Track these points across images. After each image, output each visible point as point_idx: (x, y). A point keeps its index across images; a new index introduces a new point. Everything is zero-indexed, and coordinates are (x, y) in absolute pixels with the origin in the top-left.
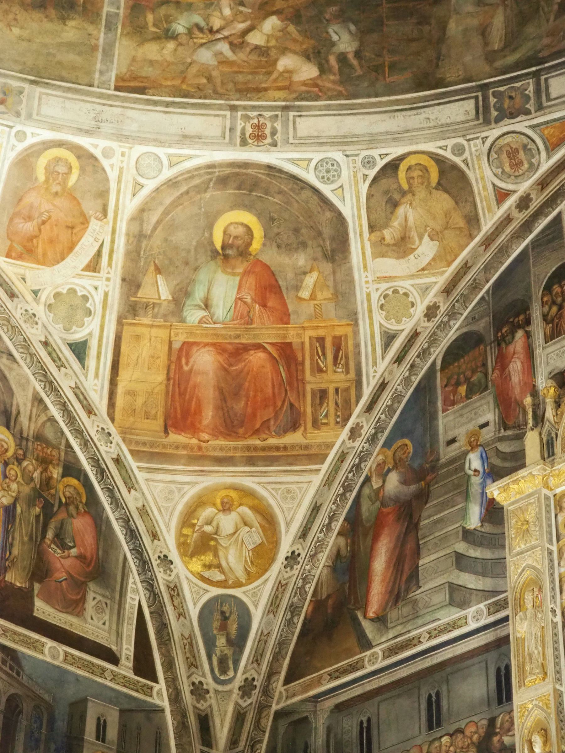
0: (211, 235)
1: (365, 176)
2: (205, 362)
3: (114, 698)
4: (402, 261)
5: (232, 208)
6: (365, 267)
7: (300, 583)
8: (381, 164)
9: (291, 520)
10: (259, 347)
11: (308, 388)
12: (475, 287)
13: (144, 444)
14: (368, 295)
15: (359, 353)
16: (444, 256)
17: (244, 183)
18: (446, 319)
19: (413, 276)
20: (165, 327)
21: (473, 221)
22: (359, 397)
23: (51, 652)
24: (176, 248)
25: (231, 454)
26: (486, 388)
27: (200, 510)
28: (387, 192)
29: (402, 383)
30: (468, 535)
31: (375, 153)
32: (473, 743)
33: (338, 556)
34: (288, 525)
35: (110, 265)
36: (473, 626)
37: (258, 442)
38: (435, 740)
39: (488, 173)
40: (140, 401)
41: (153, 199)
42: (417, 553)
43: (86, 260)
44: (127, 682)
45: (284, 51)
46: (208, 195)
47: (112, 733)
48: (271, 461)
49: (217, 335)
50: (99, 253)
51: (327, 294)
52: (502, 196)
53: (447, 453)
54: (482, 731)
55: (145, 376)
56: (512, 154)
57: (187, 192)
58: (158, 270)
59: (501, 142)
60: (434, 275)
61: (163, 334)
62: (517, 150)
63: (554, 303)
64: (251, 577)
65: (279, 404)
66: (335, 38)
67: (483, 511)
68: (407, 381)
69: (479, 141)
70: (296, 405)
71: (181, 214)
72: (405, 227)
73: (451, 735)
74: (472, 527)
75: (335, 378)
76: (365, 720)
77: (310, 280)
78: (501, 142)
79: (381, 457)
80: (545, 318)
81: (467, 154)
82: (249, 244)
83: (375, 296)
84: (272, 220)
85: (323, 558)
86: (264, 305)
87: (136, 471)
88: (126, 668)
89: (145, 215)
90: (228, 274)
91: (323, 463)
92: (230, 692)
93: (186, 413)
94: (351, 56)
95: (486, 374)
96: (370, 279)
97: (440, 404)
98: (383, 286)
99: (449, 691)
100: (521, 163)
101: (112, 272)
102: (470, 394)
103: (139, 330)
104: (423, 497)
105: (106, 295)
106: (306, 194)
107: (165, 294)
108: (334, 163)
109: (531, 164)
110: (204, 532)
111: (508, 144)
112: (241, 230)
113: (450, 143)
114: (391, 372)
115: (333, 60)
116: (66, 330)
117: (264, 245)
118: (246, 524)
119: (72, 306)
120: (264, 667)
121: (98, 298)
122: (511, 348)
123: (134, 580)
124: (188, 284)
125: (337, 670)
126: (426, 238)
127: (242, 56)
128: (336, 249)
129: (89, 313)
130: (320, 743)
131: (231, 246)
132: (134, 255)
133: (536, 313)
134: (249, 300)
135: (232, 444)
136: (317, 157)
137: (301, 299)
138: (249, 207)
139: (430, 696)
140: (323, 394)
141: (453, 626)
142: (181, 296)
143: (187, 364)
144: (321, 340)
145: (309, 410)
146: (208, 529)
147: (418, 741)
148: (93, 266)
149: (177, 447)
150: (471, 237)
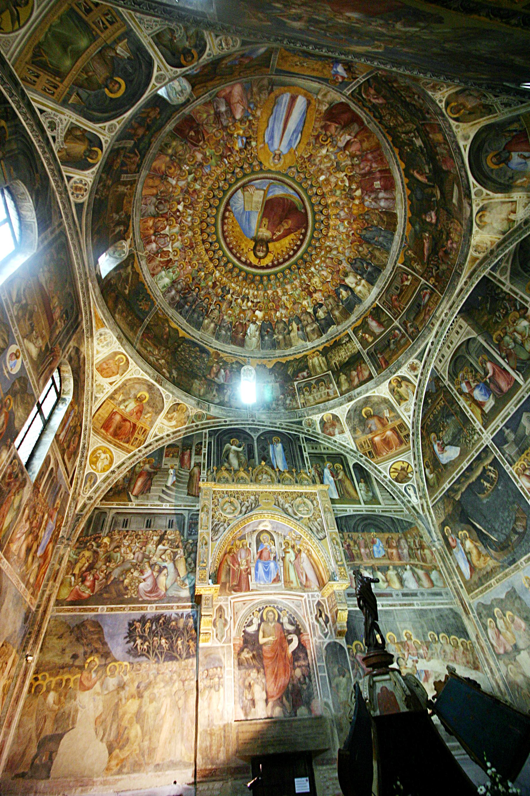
2: (118, 418)
9: (117, 462)
16: (176, 426)
29: (155, 447)
30: (166, 486)
33: (126, 476)
42: (151, 485)
48: (119, 447)
53: (163, 466)
55: (104, 414)
75: (141, 437)
77: (149, 415)
85: (121, 475)
104: (155, 473)
120: (97, 495)
121: (106, 390)
123: (79, 459)
128: (158, 413)
133: (194, 448)
142: (124, 401)
148: (111, 384)
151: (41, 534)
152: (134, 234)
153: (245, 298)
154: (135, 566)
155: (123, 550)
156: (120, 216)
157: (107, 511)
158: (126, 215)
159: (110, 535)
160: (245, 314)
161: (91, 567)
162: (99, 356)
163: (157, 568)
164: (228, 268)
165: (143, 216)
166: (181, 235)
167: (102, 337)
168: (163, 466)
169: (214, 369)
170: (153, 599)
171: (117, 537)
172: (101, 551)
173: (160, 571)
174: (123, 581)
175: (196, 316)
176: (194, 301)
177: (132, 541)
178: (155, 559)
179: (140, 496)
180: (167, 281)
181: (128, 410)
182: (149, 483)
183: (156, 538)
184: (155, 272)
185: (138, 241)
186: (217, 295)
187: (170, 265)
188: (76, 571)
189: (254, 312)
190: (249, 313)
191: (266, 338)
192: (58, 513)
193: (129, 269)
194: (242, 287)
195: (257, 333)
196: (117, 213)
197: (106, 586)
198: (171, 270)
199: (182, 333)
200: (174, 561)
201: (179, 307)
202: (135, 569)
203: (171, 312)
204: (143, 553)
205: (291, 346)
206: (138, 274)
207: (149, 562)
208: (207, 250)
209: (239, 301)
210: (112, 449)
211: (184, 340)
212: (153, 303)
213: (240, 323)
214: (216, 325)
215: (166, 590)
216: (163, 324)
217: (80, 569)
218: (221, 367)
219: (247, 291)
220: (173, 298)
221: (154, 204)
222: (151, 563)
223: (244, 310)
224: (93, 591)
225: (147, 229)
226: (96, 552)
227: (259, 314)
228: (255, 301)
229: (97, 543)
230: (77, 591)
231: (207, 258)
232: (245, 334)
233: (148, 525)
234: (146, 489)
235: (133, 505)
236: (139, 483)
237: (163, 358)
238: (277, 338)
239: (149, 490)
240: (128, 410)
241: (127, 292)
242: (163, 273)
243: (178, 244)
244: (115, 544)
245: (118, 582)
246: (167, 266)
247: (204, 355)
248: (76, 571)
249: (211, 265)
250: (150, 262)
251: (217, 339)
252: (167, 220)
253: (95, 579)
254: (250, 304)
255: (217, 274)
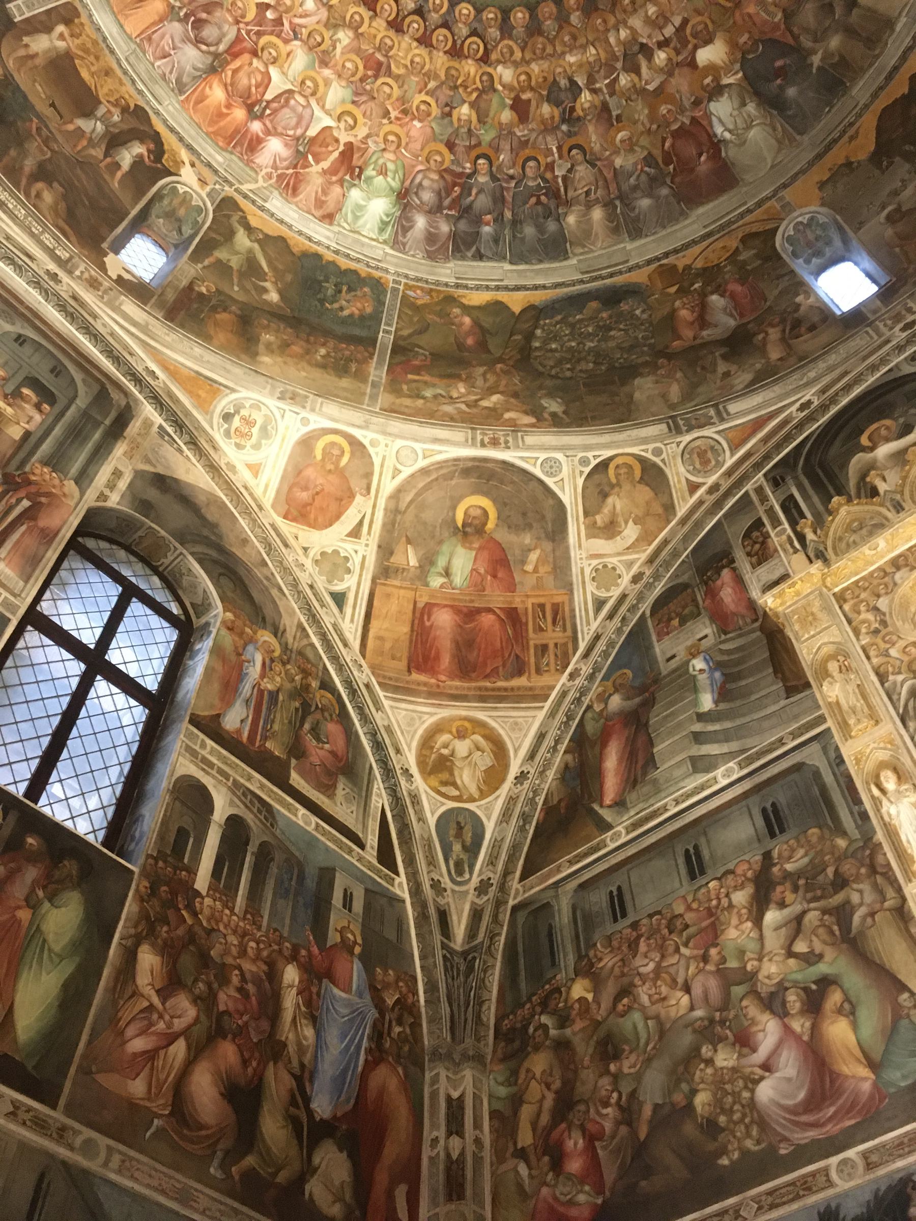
0: (454, 515)
1: (581, 472)
2: (444, 620)
3: (361, 877)
4: (610, 542)
5: (473, 493)
6: (580, 546)
7: (531, 795)
8: (594, 463)
10: (489, 610)
11: (532, 643)
12: (675, 554)
13: (390, 679)
14: (582, 569)
15: (574, 616)
16: (645, 538)
17: (482, 475)
18: (651, 580)
19: (619, 554)
20: (412, 589)
21: (670, 508)
22: (576, 649)
23: (302, 817)
24: (425, 523)
25: (465, 692)
26: (699, 614)
27: (438, 736)
28: (599, 485)
31: (590, 455)
32: (748, 879)
34: (516, 751)
35: (369, 533)
36: (724, 782)
37: (488, 684)
38: (700, 888)
39: (682, 469)
40: (388, 645)
41: (408, 482)
42: (651, 743)
43: (349, 528)
44: (371, 867)
45: (508, 410)
46: (453, 482)
47: (358, 905)
48: (501, 699)
49: (454, 600)
50: (361, 523)
51: (548, 568)
52: (693, 488)
54: (757, 867)
55: (393, 626)
56: (702, 454)
57: (437, 479)
58: (409, 541)
59: (693, 445)
60: (637, 552)
61: (410, 594)
62: (706, 451)
63: (755, 543)
64: (483, 795)
65: (507, 655)
66: (546, 405)
67: (716, 696)
68: (619, 631)
69: (674, 445)
70: (521, 656)
71: (430, 497)
72: (613, 513)
73: (719, 879)
74: (706, 709)
75: (554, 636)
76: (614, 889)
77: (534, 556)
78: (693, 445)
79: (600, 689)
80: (749, 554)
81: (664, 455)
82: (486, 524)
83: (587, 571)
84: (505, 504)
86: (494, 576)
87: (383, 699)
88: (371, 854)
89: (401, 495)
90: (466, 548)
91: (546, 701)
92: (467, 892)
93: (426, 658)
94: (561, 414)
95: (697, 606)
96: (584, 556)
97: (654, 638)
98: (595, 562)
99: (708, 841)
100: (709, 461)
101: (371, 539)
102: (683, 622)
103: (389, 590)
104: (649, 703)
105: (364, 557)
106: (533, 484)
107: (413, 562)
108: (556, 461)
109: (717, 462)
110: (442, 755)
111: (698, 447)
112: (478, 512)
113: (651, 447)
114: (604, 627)
115: (546, 415)
116: (329, 582)
117: (497, 525)
118: (478, 749)
119: (334, 564)
120: (500, 866)
121: (358, 559)
122: (719, 583)
124: (433, 555)
125: (576, 856)
126: (631, 522)
127: (474, 411)
129: (349, 571)
130: (566, 920)
131: (470, 525)
132: (390, 526)
134: (482, 571)
135: (466, 685)
136: (543, 456)
137: (526, 572)
138: (486, 494)
139: (687, 851)
140: (544, 648)
141: (702, 788)
142: (427, 562)
143: (429, 620)
144: (542, 606)
145: (532, 660)
146: (445, 752)
147: (682, 892)
148: (355, 533)
149: (419, 684)
150: (669, 522)
151: (295, 1032)
152: (190, 148)
153: (635, 54)
154: (709, 1032)
155: (644, 994)
156: (104, 119)
157: (547, 897)
158: (125, 110)
159: (586, 968)
160: (670, 99)
161: (566, 1104)
162: (263, 478)
163: (792, 998)
164: (519, 31)
165: (180, 87)
166: (324, 63)
167: (236, 422)
168: (665, 669)
169: (684, 314)
170: (832, 1129)
171: (608, 961)
172: (576, 1030)
173: (814, 1003)
174: (689, 1107)
175: (529, 231)
176: (499, 199)
177: (662, 948)
178: (771, 970)
179: (631, 797)
180: (379, 207)
181: (458, 579)
182: (641, 740)
183: (740, 898)
184: (330, 207)
185: (218, 158)
186: (548, 128)
187: (356, 161)
188: (525, 1138)
189: (692, 64)
190: (681, 84)
191: (791, 92)
192: (367, 961)
193: (242, 240)
194: (601, 39)
195: (751, 108)
196: (88, 114)
197: (640, 1149)
198: (370, 172)
199: (516, 302)
200: (854, 944)
201: (463, 244)
202: (716, 1042)
203: (447, 272)
204: (721, 973)
205: (889, 24)
206: (282, 239)
207: (754, 993)
208: (424, 40)
209: (624, 80)
210: (481, 716)
211: (535, 313)
212: (378, 286)
213: (676, 135)
214: (608, 205)
215: (873, 1065)
216: (444, 315)
217: (534, 1125)
218: (703, 295)
219: (623, 34)
220: (431, 237)
221: (186, 39)
222: (763, 990)
223: (660, 90)
224: (599, 1189)
225: (221, 115)
226: (562, 1046)
227: (710, 54)
228: (669, 31)
229: (554, 1013)
230: (551, 1210)
231: (440, 61)
232: (715, 146)
233: (696, 867)
234: (640, 766)
235: (619, 835)
236: (612, 762)
237: (491, 391)
238: (826, 57)
239: (651, 762)
240: (458, 579)
241: (273, 296)
242: (355, 194)
243: (337, 93)
244: (610, 989)
245: (674, 1115)
246: (351, 170)
247: (624, 307)
248: (525, 1138)
249: (470, 67)
250: (295, 191)
251: (636, 232)
252: (255, 53)
253: (591, 1139)
254: (661, 57)
255: (505, 74)
